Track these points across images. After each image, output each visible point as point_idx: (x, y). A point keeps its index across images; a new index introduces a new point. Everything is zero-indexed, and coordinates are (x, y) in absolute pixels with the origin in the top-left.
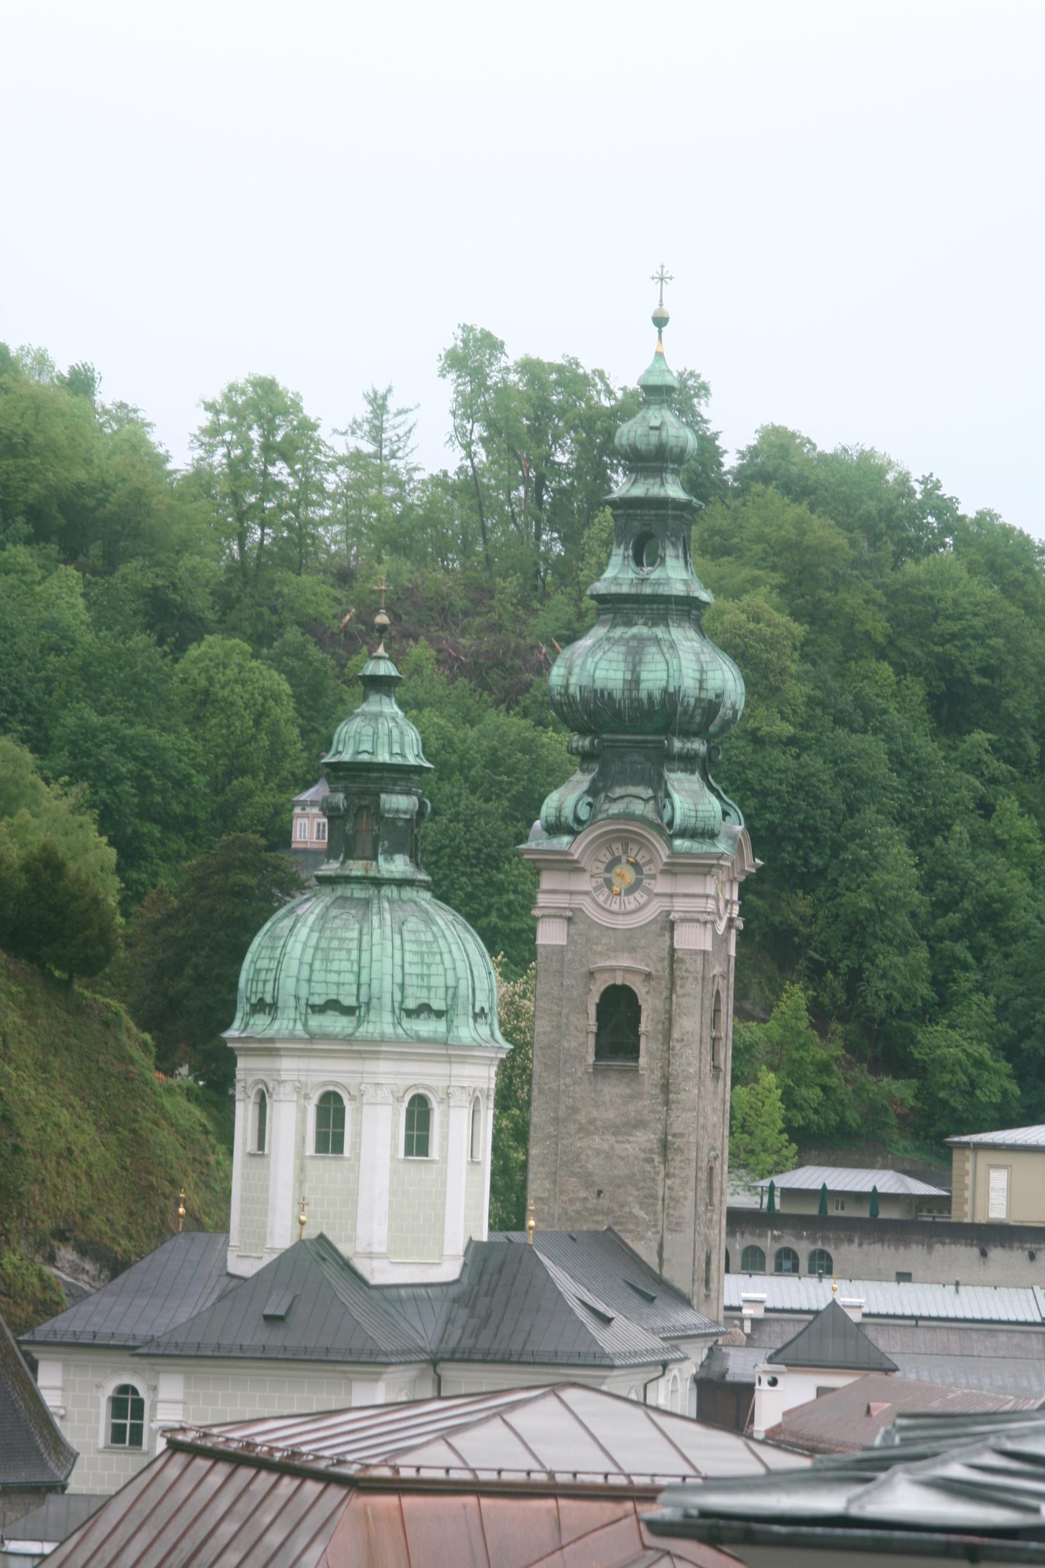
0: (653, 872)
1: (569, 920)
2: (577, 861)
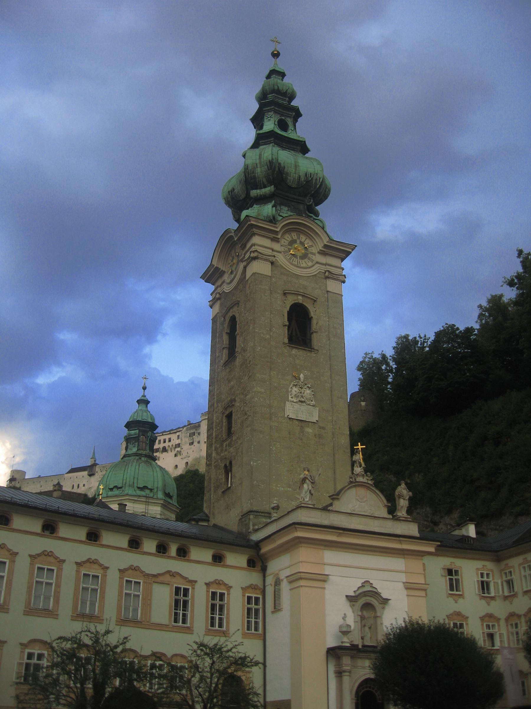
0: (314, 251)
1: (272, 263)
2: (276, 233)
